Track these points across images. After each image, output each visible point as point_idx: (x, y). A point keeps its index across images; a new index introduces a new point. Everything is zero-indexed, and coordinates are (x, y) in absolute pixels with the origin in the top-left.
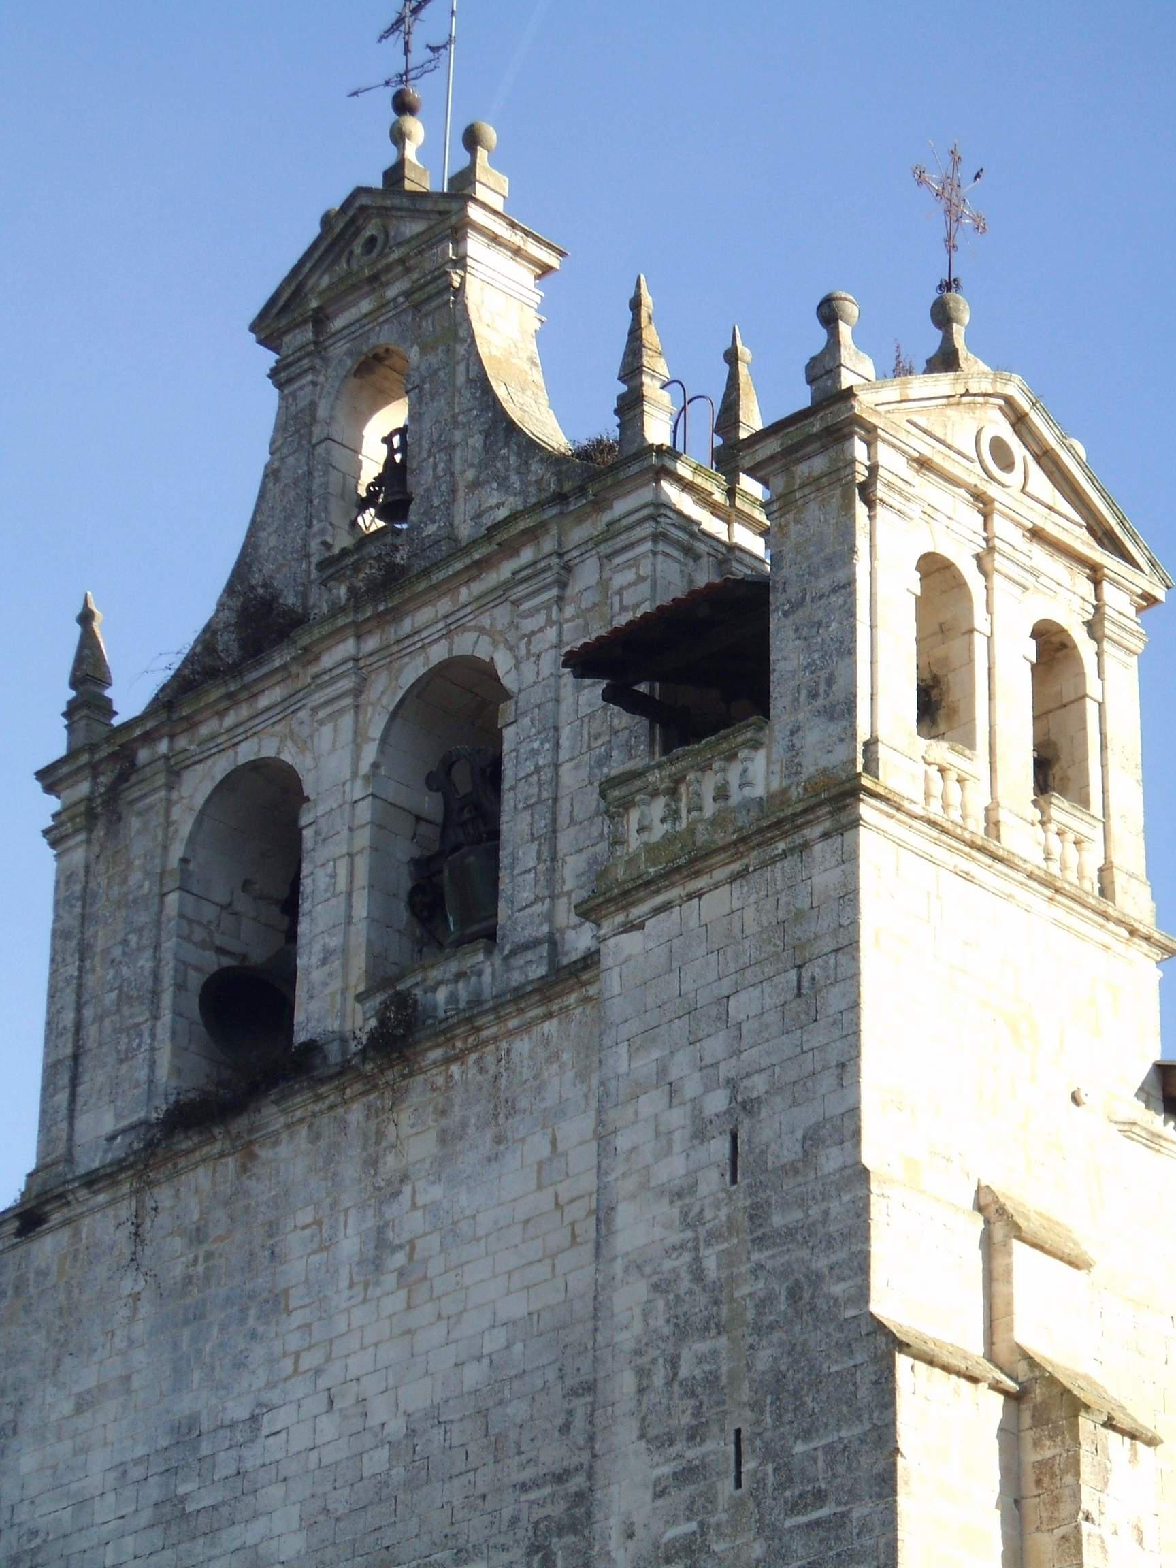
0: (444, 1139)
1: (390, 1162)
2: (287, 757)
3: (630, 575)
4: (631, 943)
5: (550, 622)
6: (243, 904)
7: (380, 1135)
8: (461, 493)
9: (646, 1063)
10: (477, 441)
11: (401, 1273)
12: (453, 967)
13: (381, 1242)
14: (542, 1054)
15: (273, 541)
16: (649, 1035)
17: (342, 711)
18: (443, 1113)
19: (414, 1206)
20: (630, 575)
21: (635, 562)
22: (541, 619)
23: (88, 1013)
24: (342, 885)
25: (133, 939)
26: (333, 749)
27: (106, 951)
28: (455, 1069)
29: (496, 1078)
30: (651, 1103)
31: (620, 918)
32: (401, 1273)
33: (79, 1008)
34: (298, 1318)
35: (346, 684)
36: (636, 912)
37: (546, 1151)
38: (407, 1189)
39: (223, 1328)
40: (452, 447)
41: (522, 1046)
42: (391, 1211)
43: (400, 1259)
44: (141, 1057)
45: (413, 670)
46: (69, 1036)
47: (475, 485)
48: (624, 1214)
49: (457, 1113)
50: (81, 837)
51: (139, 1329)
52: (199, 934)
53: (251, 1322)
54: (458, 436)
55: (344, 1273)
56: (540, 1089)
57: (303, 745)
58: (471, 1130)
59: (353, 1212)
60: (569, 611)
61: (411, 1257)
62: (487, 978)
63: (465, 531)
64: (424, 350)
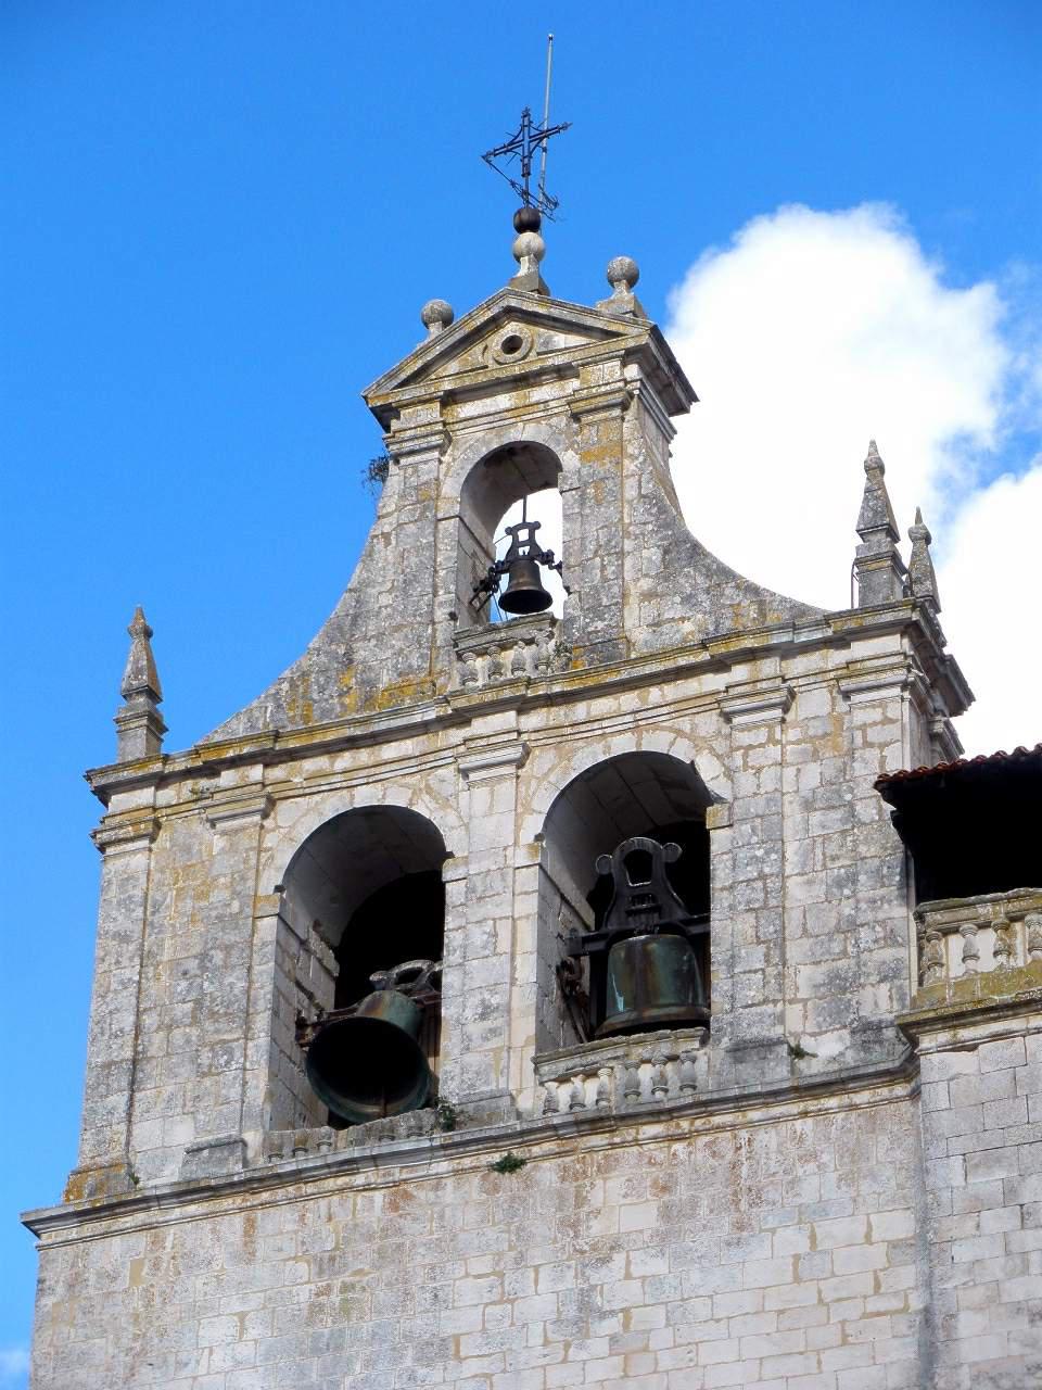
0: (666, 1213)
1: (596, 1227)
2: (420, 809)
3: (876, 715)
4: (962, 1062)
5: (771, 740)
6: (315, 943)
7: (580, 1200)
8: (633, 601)
9: (989, 1182)
10: (654, 554)
11: (613, 1339)
12: (665, 1048)
13: (587, 1310)
14: (793, 1151)
15: (385, 600)
16: (989, 1156)
17: (501, 778)
18: (665, 1189)
19: (628, 1276)
20: (876, 715)
21: (882, 703)
22: (763, 732)
23: (149, 1020)
24: (504, 945)
25: (218, 957)
26: (489, 812)
27: (175, 963)
28: (678, 1147)
29: (734, 1166)
30: (998, 1221)
31: (944, 1037)
32: (613, 1339)
33: (138, 1014)
34: (472, 1367)
35: (514, 753)
36: (965, 1034)
37: (803, 1246)
38: (619, 1259)
39: (369, 1363)
40: (621, 554)
41: (767, 1139)
42: (596, 1277)
43: (612, 1325)
44: (231, 1075)
45: (588, 756)
46: (129, 1039)
47: (648, 596)
48: (967, 1324)
49: (682, 1192)
50: (145, 843)
51: (245, 1350)
52: (288, 966)
53: (408, 1362)
54: (628, 545)
55: (536, 1330)
56: (793, 1183)
57: (445, 803)
58: (703, 1211)
59: (544, 1273)
60: (792, 734)
61: (626, 1325)
62: (701, 1065)
63: (640, 635)
64: (585, 456)
